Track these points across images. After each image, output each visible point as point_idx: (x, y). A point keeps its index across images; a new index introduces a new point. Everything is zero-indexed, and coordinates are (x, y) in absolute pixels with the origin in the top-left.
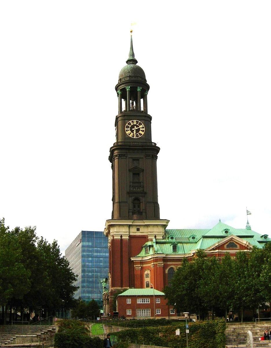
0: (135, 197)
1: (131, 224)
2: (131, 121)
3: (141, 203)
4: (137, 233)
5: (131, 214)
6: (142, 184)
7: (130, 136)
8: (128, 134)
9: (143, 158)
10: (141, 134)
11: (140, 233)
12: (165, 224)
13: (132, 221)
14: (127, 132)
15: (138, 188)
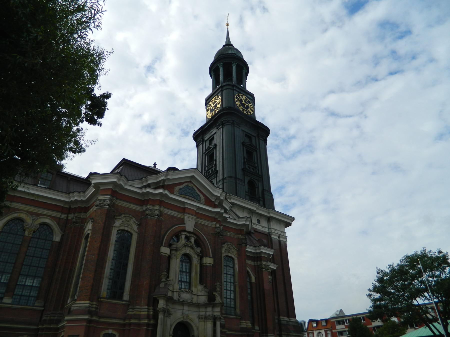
0: (251, 178)
1: (255, 209)
2: (240, 94)
3: (256, 189)
4: (258, 226)
5: (248, 197)
6: (256, 165)
7: (240, 108)
8: (238, 105)
9: (255, 137)
10: (250, 113)
11: (261, 227)
12: (290, 221)
13: (257, 205)
14: (237, 103)
15: (252, 169)
